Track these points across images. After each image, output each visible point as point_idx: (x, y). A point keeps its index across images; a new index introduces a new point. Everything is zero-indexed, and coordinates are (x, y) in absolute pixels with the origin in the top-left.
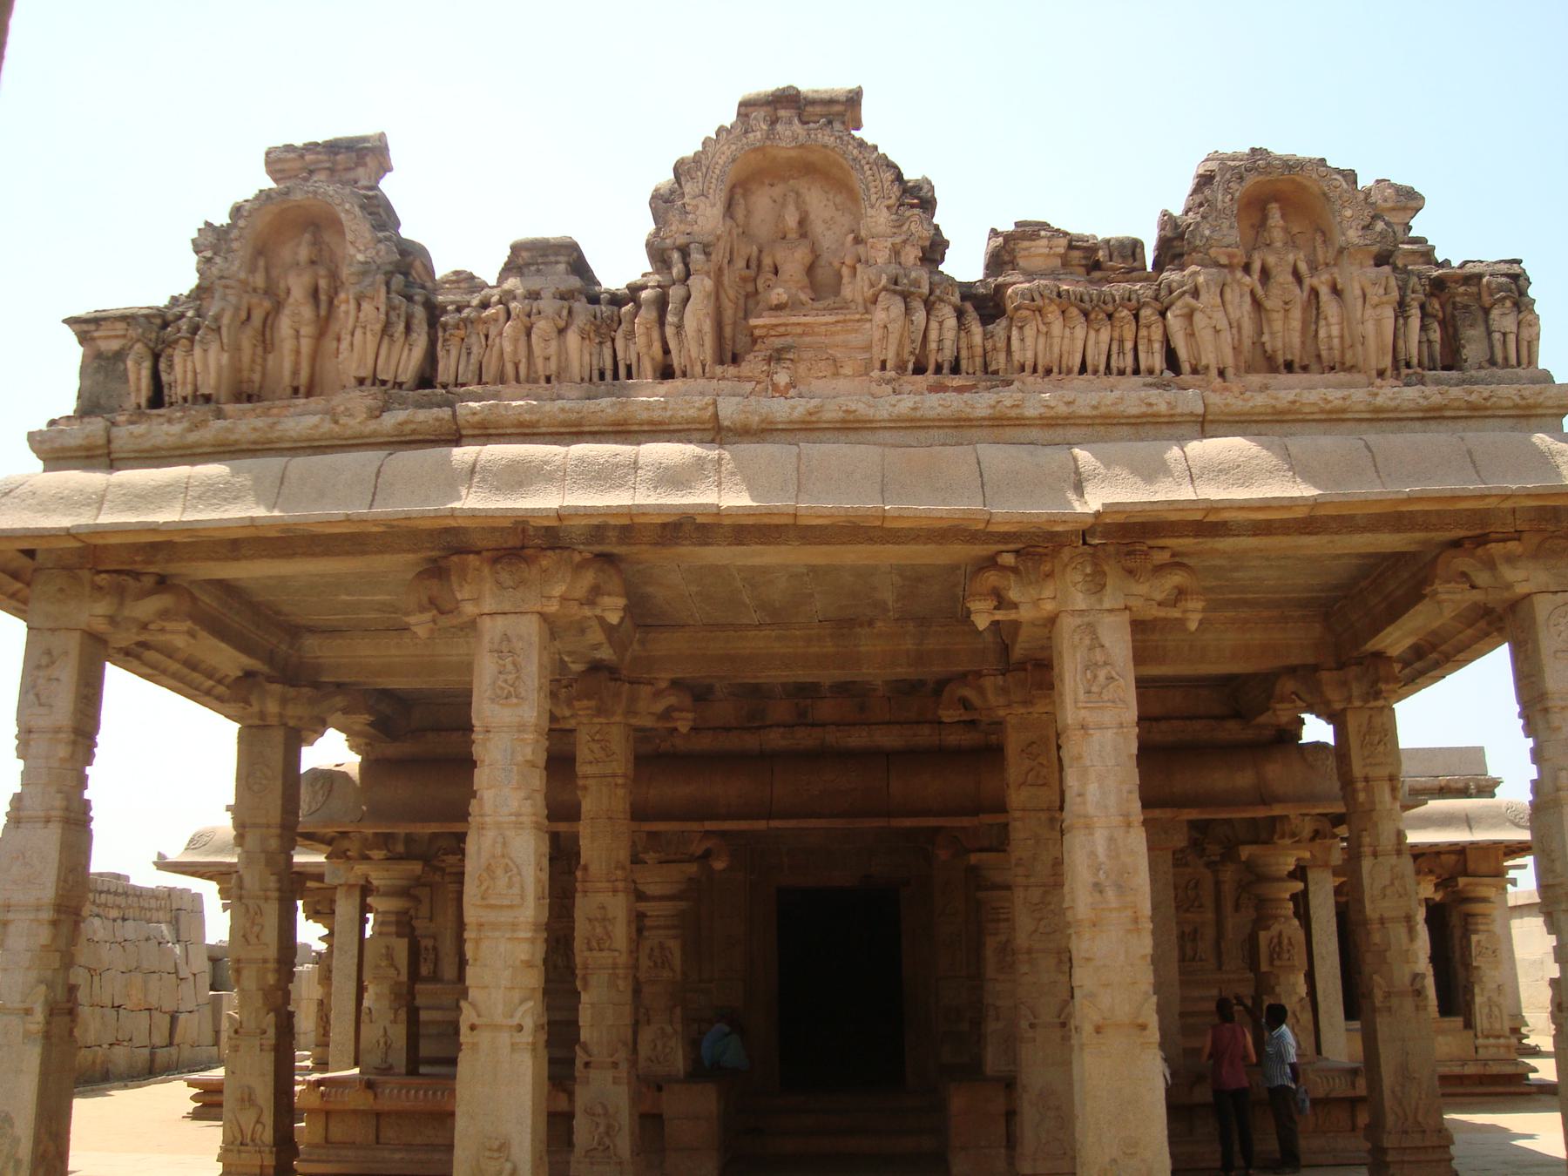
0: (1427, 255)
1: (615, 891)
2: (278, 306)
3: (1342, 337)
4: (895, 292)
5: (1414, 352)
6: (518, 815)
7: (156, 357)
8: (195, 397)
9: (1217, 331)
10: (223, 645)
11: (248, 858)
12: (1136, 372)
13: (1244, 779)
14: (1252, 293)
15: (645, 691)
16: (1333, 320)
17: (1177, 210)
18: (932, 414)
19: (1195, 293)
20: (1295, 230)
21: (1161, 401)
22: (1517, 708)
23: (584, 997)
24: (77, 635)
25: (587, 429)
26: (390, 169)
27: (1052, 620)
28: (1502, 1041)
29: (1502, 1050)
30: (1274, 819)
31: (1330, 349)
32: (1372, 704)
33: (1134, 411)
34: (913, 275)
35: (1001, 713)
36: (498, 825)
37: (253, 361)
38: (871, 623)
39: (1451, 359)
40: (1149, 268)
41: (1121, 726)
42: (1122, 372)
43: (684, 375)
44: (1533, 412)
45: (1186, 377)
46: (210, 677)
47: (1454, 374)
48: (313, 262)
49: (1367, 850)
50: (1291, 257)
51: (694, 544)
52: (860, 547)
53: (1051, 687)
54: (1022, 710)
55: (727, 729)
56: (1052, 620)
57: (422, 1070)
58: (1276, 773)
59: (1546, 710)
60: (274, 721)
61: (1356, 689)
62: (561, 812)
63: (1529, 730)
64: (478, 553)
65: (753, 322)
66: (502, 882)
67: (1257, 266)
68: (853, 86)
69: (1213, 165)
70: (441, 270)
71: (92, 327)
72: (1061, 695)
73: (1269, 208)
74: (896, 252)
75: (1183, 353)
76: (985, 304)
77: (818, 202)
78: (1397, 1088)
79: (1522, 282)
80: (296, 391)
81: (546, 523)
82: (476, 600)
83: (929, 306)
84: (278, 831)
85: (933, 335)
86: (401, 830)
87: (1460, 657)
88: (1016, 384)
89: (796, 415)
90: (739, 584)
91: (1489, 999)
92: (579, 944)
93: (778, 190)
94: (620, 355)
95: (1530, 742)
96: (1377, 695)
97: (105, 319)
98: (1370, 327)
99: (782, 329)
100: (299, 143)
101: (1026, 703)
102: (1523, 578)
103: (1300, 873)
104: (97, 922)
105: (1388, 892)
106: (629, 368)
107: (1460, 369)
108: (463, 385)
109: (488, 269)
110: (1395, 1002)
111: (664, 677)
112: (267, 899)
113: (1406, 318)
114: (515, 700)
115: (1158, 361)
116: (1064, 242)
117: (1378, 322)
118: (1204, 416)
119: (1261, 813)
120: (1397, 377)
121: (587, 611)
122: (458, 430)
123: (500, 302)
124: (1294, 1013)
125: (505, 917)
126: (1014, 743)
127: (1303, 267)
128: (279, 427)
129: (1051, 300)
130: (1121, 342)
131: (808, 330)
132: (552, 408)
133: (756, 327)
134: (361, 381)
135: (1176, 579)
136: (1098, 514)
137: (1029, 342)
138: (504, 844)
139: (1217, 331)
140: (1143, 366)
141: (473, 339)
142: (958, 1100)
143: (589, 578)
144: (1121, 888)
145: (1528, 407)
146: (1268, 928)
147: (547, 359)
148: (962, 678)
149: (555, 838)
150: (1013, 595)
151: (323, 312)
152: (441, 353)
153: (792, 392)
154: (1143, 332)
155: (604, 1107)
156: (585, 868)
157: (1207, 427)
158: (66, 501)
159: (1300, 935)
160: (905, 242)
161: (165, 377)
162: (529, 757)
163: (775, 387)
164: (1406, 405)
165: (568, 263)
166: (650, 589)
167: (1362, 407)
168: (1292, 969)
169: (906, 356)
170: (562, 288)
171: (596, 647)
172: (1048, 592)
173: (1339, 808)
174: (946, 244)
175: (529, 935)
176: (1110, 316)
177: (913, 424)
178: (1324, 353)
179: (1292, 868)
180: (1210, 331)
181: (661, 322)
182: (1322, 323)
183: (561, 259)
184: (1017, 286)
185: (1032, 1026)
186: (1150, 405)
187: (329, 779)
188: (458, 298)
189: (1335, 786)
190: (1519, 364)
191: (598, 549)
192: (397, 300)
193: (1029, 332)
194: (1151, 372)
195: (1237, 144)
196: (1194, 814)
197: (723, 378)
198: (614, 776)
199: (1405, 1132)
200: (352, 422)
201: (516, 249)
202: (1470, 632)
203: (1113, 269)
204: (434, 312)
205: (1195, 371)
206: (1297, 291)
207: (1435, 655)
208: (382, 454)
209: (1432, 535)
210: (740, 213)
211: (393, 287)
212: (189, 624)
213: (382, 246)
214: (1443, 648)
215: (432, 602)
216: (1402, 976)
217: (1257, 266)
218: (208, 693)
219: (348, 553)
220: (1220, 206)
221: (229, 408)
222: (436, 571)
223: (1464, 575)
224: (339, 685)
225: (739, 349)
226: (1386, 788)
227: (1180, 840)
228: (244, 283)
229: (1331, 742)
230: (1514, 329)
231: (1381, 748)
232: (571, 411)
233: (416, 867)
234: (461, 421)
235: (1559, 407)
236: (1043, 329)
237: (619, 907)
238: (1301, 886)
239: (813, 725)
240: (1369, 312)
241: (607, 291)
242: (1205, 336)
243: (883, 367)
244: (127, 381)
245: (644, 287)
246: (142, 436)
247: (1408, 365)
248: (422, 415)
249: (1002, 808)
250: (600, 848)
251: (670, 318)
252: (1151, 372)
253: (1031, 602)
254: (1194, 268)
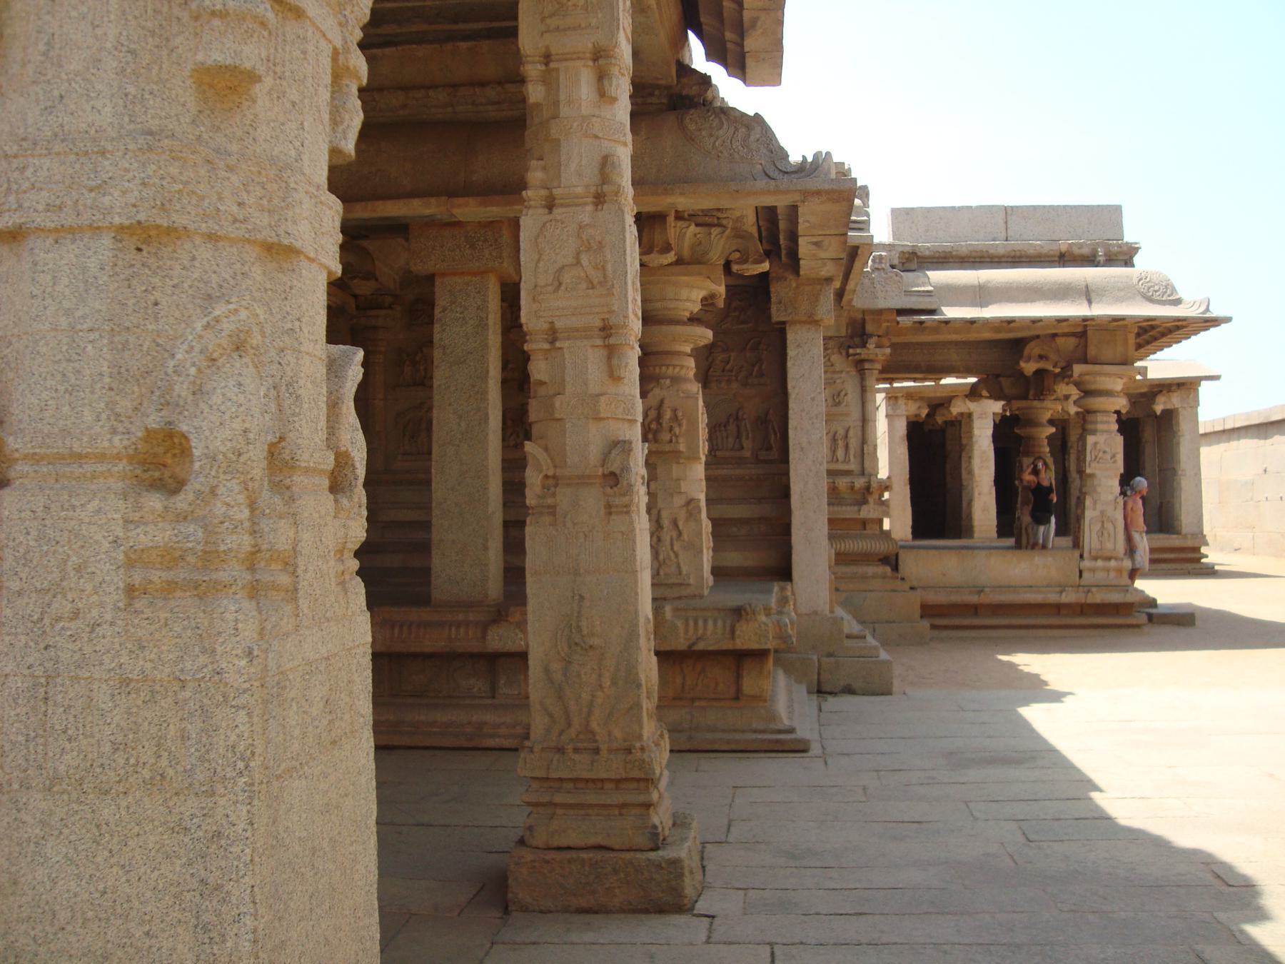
28: (1113, 563)
29: (1112, 575)
78: (556, 666)
91: (1102, 512)
105: (567, 277)
110: (563, 497)
124: (675, 523)
199: (560, 750)
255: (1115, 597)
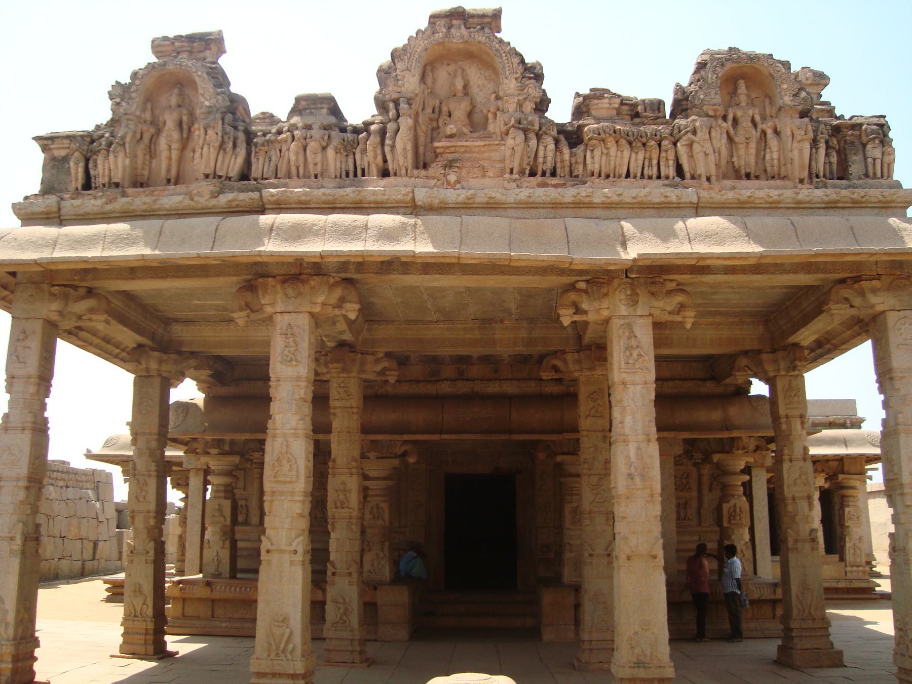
0: (831, 112)
1: (351, 474)
2: (159, 132)
3: (779, 159)
4: (519, 128)
5: (821, 169)
6: (295, 429)
7: (87, 160)
8: (110, 184)
9: (706, 155)
10: (125, 329)
11: (139, 452)
12: (659, 177)
13: (716, 415)
14: (728, 133)
15: (371, 358)
16: (775, 149)
17: (685, 83)
18: (539, 200)
19: (694, 132)
20: (754, 96)
21: (673, 195)
22: (875, 377)
23: (333, 535)
24: (41, 322)
25: (338, 206)
26: (225, 52)
27: (607, 321)
28: (861, 568)
29: (861, 574)
30: (733, 439)
31: (772, 166)
32: (792, 373)
33: (657, 200)
34: (530, 118)
35: (576, 374)
36: (284, 435)
37: (144, 163)
38: (502, 321)
39: (843, 174)
40: (668, 117)
41: (646, 383)
42: (650, 178)
43: (395, 175)
44: (890, 205)
45: (688, 181)
46: (118, 348)
47: (844, 182)
48: (179, 106)
49: (786, 457)
50: (751, 112)
51: (399, 274)
52: (495, 277)
53: (606, 360)
54: (588, 373)
55: (418, 382)
56: (607, 321)
57: (239, 575)
58: (735, 412)
59: (891, 379)
60: (154, 373)
61: (782, 365)
62: (320, 428)
63: (882, 390)
64: (274, 277)
65: (436, 144)
66: (286, 467)
67: (730, 117)
68: (497, 7)
69: (706, 57)
70: (254, 112)
71: (50, 142)
72: (611, 364)
73: (739, 82)
74: (520, 105)
75: (686, 167)
76: (571, 136)
77: (475, 75)
79: (885, 128)
80: (169, 181)
81: (314, 260)
82: (273, 304)
83: (539, 137)
84: (156, 437)
85: (541, 154)
86: (228, 437)
87: (844, 347)
88: (589, 183)
89: (460, 199)
90: (425, 297)
91: (854, 544)
92: (330, 505)
93: (451, 68)
94: (358, 162)
95: (882, 397)
96: (794, 368)
97: (57, 137)
98: (796, 152)
99: (453, 149)
100: (171, 35)
101: (591, 369)
102: (880, 301)
103: (747, 470)
104: (51, 488)
105: (798, 482)
106: (363, 170)
107: (848, 179)
108: (266, 179)
109: (282, 112)
110: (800, 545)
111: (381, 351)
112: (150, 476)
113: (817, 149)
114: (294, 363)
115: (672, 172)
116: (618, 101)
117: (801, 150)
118: (698, 204)
119: (725, 435)
120: (811, 183)
121: (337, 312)
122: (263, 205)
123: (289, 131)
124: (742, 551)
125: (287, 488)
126: (583, 392)
127: (758, 118)
128: (159, 202)
129: (610, 135)
130: (650, 159)
131: (468, 150)
132: (318, 193)
133: (437, 147)
134: (207, 176)
135: (679, 298)
136: (634, 260)
137: (597, 159)
138: (288, 446)
139: (706, 155)
140: (663, 174)
141: (273, 152)
142: (547, 598)
143: (338, 293)
144: (643, 476)
145: (887, 202)
146: (728, 502)
147: (316, 164)
148: (554, 354)
149: (317, 443)
150: (585, 306)
151: (185, 136)
152: (253, 160)
153: (458, 186)
154: (663, 154)
155: (344, 598)
156: (334, 461)
157: (699, 210)
158: (33, 244)
159: (747, 505)
160: (525, 99)
161: (92, 172)
162: (303, 396)
163: (448, 183)
164: (816, 199)
165: (328, 108)
166: (372, 299)
167: (790, 200)
168: (741, 525)
169: (525, 166)
170: (325, 123)
171: (342, 332)
172: (605, 304)
173: (770, 433)
174: (549, 101)
175: (301, 498)
176: (644, 145)
177: (528, 206)
178: (769, 169)
179: (743, 467)
180: (702, 154)
181: (383, 144)
182: (768, 151)
183: (324, 106)
184: (590, 126)
185: (591, 555)
186: (666, 197)
187: (186, 407)
188: (264, 128)
189: (768, 420)
190: (882, 177)
191: (344, 275)
192: (228, 129)
193: (597, 153)
194: (667, 178)
195: (721, 45)
196: (687, 435)
197: (418, 177)
198: (352, 407)
199: (803, 620)
200: (202, 200)
201: (298, 100)
202: (849, 332)
203: (646, 117)
204: (250, 136)
205: (693, 178)
206: (754, 131)
207: (828, 346)
208: (219, 218)
209: (828, 276)
210: (429, 80)
211: (226, 121)
212: (106, 316)
213: (220, 97)
214: (834, 341)
215: (247, 305)
216: (804, 530)
217: (730, 117)
218: (116, 357)
219: (199, 276)
220: (710, 81)
221: (130, 191)
222: (250, 287)
223: (846, 299)
224: (192, 353)
225: (428, 160)
226: (798, 422)
227: (679, 450)
228: (139, 117)
229: (767, 395)
230: (880, 156)
231: (796, 399)
232: (329, 195)
233: (236, 459)
234: (265, 200)
235: (906, 202)
236: (605, 151)
237: (353, 483)
238: (747, 478)
239: (467, 380)
240: (795, 145)
241: (351, 125)
242: (699, 157)
243: (511, 172)
244: (70, 174)
245: (373, 123)
246: (79, 206)
247: (817, 176)
248: (243, 196)
249: (575, 430)
250: (342, 449)
251: (388, 142)
252: (667, 178)
253: (594, 310)
254: (693, 117)
255: (864, 585)
